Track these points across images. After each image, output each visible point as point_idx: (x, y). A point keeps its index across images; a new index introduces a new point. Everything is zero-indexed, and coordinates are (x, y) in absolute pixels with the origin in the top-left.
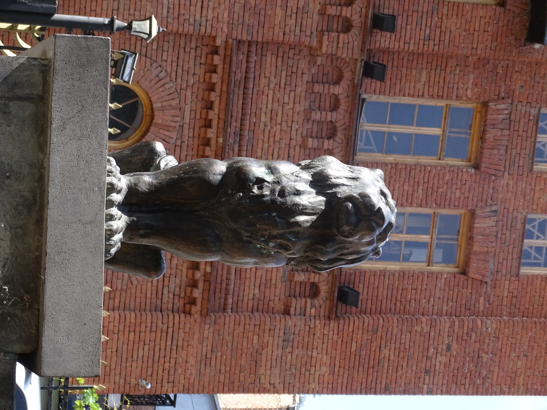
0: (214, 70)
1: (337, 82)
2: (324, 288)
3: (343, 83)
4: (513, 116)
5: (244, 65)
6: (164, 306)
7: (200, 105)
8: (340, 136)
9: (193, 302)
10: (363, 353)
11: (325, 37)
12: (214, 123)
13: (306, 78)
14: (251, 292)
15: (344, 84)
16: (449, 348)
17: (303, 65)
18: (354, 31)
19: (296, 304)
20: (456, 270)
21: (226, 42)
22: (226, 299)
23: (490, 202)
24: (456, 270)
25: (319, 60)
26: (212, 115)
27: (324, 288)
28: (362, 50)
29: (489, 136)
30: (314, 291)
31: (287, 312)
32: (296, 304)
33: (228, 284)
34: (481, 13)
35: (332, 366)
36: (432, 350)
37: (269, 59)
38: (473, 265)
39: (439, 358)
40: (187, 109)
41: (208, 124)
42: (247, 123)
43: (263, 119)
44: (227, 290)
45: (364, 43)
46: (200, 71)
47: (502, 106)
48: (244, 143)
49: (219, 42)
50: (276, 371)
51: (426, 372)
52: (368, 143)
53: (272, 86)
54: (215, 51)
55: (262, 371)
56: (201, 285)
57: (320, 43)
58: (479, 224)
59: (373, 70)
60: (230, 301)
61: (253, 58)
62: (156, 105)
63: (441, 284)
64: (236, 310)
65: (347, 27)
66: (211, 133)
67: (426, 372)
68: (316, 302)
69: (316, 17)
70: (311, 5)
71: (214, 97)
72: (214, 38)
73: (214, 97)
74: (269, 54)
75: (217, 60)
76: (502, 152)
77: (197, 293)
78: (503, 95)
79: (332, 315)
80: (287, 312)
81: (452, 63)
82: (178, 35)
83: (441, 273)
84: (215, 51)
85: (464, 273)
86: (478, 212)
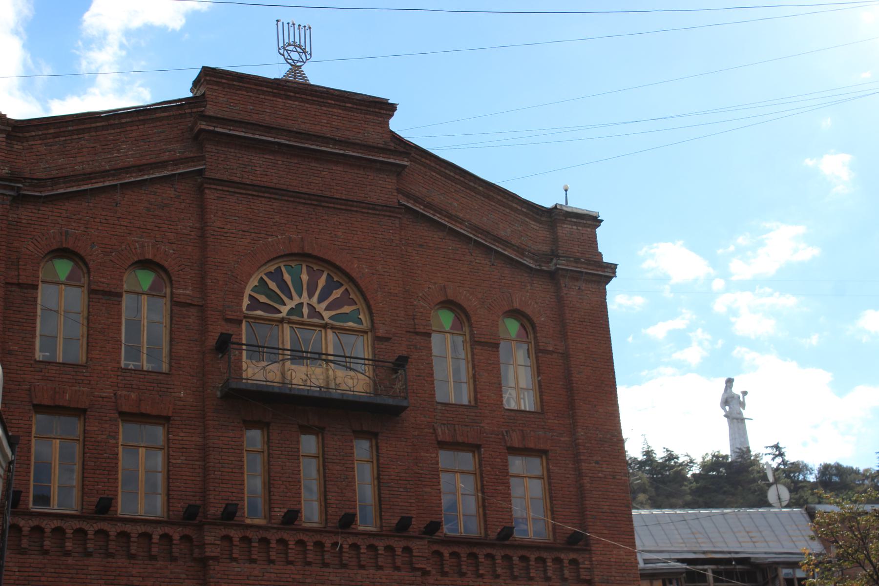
4: (445, 422)
8: (475, 550)
10: (609, 525)
11: (417, 566)
13: (439, 578)
16: (597, 463)
19: (584, 575)
20: (544, 458)
23: (500, 436)
24: (544, 458)
27: (572, 556)
30: (574, 562)
32: (584, 575)
39: (604, 469)
47: (440, 430)
51: (614, 478)
58: (516, 444)
59: (433, 527)
65: (407, 550)
67: (614, 478)
68: (581, 561)
69: (403, 573)
70: (396, 577)
78: (431, 430)
86: (508, 445)
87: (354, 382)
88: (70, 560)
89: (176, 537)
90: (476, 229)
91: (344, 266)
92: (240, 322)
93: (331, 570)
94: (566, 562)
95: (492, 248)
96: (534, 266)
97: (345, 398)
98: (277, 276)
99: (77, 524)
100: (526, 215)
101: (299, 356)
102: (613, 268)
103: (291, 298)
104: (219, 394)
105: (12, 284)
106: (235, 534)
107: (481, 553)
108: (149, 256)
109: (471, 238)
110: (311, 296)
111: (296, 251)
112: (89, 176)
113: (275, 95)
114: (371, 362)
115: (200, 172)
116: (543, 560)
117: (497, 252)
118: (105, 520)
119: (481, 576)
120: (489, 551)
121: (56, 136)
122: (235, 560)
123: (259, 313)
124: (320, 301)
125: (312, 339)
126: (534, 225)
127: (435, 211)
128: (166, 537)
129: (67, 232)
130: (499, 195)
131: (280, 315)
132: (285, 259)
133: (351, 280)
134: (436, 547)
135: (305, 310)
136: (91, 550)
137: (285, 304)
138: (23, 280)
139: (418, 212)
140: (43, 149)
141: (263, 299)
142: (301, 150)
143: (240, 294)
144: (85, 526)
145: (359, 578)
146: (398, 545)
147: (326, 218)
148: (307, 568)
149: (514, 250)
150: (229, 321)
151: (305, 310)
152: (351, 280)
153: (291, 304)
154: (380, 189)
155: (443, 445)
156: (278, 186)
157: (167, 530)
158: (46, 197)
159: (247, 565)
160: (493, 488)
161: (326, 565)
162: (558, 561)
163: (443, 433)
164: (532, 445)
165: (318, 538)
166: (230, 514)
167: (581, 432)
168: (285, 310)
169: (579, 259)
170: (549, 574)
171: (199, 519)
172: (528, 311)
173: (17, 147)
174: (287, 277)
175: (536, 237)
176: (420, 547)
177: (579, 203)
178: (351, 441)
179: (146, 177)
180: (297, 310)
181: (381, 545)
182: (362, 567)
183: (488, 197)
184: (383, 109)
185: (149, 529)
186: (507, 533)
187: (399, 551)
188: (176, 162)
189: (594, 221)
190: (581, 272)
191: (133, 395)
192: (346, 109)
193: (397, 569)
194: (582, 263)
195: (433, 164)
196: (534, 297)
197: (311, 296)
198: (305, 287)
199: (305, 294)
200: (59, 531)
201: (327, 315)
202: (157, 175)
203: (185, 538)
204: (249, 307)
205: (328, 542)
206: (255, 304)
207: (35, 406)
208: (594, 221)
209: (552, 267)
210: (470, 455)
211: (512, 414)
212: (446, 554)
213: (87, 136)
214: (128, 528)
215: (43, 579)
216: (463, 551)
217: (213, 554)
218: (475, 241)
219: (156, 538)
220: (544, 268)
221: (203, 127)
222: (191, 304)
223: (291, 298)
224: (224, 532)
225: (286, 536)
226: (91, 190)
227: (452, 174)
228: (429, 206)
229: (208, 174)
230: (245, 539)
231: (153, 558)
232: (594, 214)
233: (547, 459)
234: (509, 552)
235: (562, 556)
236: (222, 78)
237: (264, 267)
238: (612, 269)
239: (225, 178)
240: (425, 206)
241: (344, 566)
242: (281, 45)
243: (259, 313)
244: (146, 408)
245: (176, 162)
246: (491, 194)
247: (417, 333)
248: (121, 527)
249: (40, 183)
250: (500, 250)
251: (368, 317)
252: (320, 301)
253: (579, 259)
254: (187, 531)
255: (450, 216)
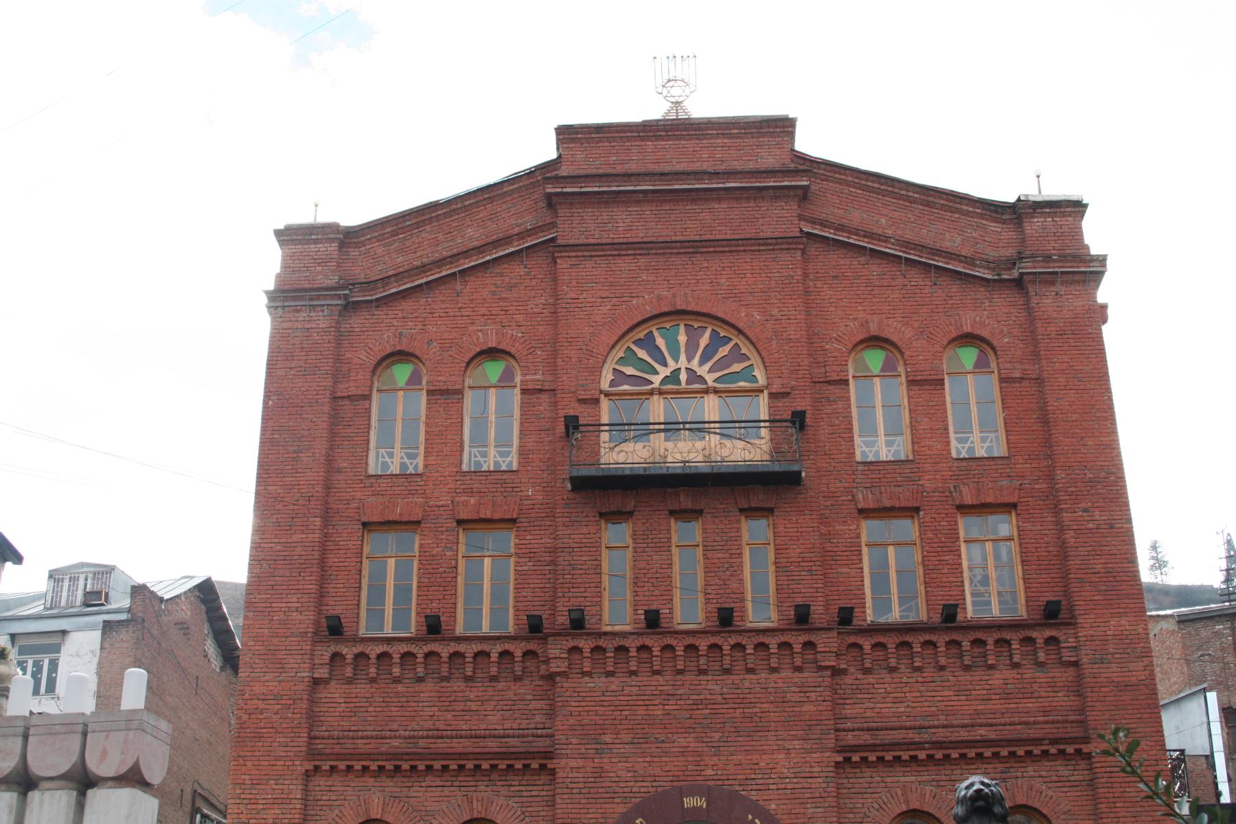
0: (864, 759)
1: (860, 647)
2: (1049, 633)
3: (861, 642)
5: (856, 733)
6: (1087, 778)
7: (898, 769)
8: (908, 638)
9: (1078, 751)
12: (912, 753)
13: (860, 676)
14: (1063, 700)
15: (860, 640)
16: (1085, 510)
17: (848, 680)
18: (812, 638)
19: (1067, 656)
20: (1013, 514)
21: (838, 752)
22: (1072, 722)
25: (843, 666)
26: (905, 756)
27: (1049, 633)
28: (828, 629)
29: (888, 504)
31: (1076, 664)
33: (1058, 722)
34: (781, 528)
35: (1119, 615)
36: (1090, 526)
37: (848, 711)
38: (1007, 499)
40: (903, 779)
41: (914, 758)
42: (908, 724)
43: (902, 710)
44: (1063, 722)
45: (822, 629)
46: (868, 772)
47: (860, 496)
48: (926, 724)
49: (840, 759)
50: (1132, 666)
52: (909, 609)
53: (872, 705)
54: (847, 760)
55: (1133, 679)
56: (1062, 747)
57: (827, 668)
58: (968, 500)
59: (846, 617)
60: (1072, 718)
61: (849, 725)
62: (904, 808)
63: (1028, 526)
64: (1082, 710)
65: (809, 645)
66: (922, 755)
69: (806, 674)
70: (796, 680)
71: (889, 757)
72: (837, 763)
73: (889, 757)
74: (844, 712)
75: (856, 758)
76: (900, 489)
77: (1070, 749)
79: (1071, 623)
80: (1076, 664)
81: (828, 546)
82: (838, 796)
83: (1018, 527)
84: (847, 760)
85: (1014, 506)
87: (748, 451)
88: (400, 688)
89: (518, 654)
90: (907, 245)
91: (727, 318)
92: (596, 401)
93: (710, 677)
94: (1040, 641)
95: (930, 265)
96: (990, 277)
97: (715, 471)
98: (647, 342)
99: (404, 648)
100: (981, 216)
101: (671, 428)
102: (1102, 260)
103: (665, 364)
104: (569, 486)
105: (342, 398)
106: (586, 644)
107: (916, 641)
108: (492, 344)
109: (900, 257)
110: (689, 360)
111: (665, 309)
112: (423, 269)
113: (642, 139)
114: (767, 424)
115: (553, 240)
116: (957, 644)
117: (937, 267)
118: (435, 640)
119: (918, 669)
120: (927, 637)
121: (395, 234)
122: (589, 674)
123: (625, 387)
124: (701, 363)
125: (686, 409)
126: (994, 227)
127: (850, 232)
128: (505, 654)
129: (401, 334)
130: (941, 198)
131: (650, 387)
132: (657, 321)
133: (740, 331)
134: (852, 639)
135: (683, 377)
136: (421, 675)
137: (657, 373)
138: (353, 391)
139: (827, 238)
140: (380, 251)
141: (630, 371)
142: (670, 192)
143: (597, 371)
144: (413, 648)
145: (747, 684)
146: (797, 640)
147: (706, 265)
148: (678, 677)
149: (960, 261)
150: (582, 401)
151: (683, 377)
152: (740, 331)
153: (664, 372)
154: (778, 219)
155: (865, 513)
156: (645, 240)
157: (508, 646)
158: (377, 300)
159: (603, 679)
160: (941, 557)
161: (702, 672)
162: (1029, 641)
163: (865, 499)
164: (990, 499)
165: (690, 640)
166: (578, 623)
167: (1060, 475)
168: (656, 380)
169: (1050, 257)
170: (1016, 659)
171: (552, 633)
172: (984, 333)
173: (354, 253)
174: (660, 342)
175: (998, 241)
176: (827, 642)
177: (1053, 190)
178: (739, 521)
179: (488, 258)
180: (674, 377)
181: (773, 642)
182: (751, 671)
183: (927, 204)
184: (783, 127)
185: (485, 647)
186: (950, 614)
187: (797, 648)
188: (521, 236)
189: (1077, 208)
190: (1056, 273)
191: (472, 500)
192: (730, 136)
193: (799, 669)
194: (1055, 261)
195: (850, 179)
196: (991, 314)
197: (689, 360)
198: (683, 350)
199: (683, 357)
200: (383, 656)
201: (710, 379)
202: (501, 253)
203: (528, 654)
204: (613, 383)
205: (703, 644)
206: (619, 377)
207: (364, 524)
208: (1077, 208)
209: (1015, 274)
210: (908, 522)
211: (964, 464)
212: (867, 647)
213: (428, 228)
214: (462, 648)
215: (371, 709)
216: (891, 641)
217: (558, 670)
218: (906, 259)
219: (494, 656)
220: (1005, 277)
221: (548, 190)
222: (540, 391)
223: (665, 364)
224: (572, 643)
225: (648, 641)
226: (427, 283)
227: (876, 185)
228: (840, 228)
229: (560, 242)
230: (598, 649)
231: (494, 679)
232: (1075, 198)
233: (1017, 515)
234: (956, 636)
235: (1034, 634)
236: (577, 133)
237: (631, 335)
238: (1102, 260)
239: (580, 242)
240: (836, 229)
241: (727, 671)
242: (659, 82)
243: (625, 387)
244: (486, 513)
245: (521, 236)
246: (931, 199)
247: (829, 382)
248: (454, 647)
249: (370, 285)
250: (940, 264)
251: (763, 372)
252: (701, 363)
253: (1050, 257)
254: (532, 646)
255: (870, 236)
